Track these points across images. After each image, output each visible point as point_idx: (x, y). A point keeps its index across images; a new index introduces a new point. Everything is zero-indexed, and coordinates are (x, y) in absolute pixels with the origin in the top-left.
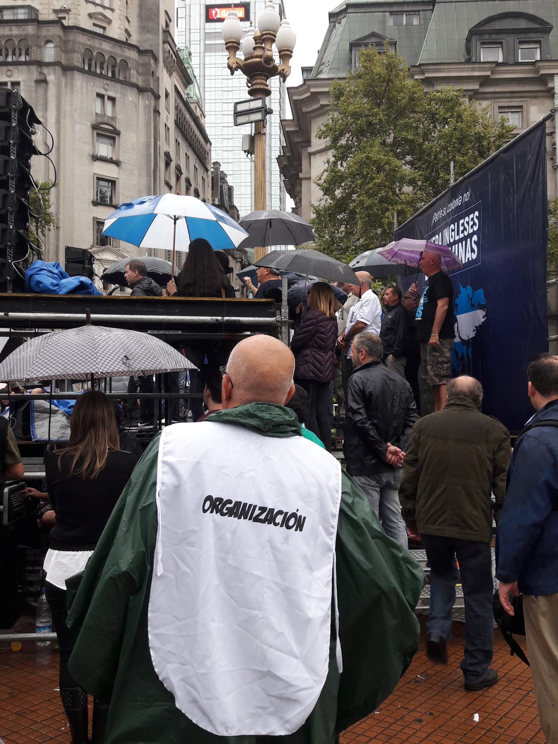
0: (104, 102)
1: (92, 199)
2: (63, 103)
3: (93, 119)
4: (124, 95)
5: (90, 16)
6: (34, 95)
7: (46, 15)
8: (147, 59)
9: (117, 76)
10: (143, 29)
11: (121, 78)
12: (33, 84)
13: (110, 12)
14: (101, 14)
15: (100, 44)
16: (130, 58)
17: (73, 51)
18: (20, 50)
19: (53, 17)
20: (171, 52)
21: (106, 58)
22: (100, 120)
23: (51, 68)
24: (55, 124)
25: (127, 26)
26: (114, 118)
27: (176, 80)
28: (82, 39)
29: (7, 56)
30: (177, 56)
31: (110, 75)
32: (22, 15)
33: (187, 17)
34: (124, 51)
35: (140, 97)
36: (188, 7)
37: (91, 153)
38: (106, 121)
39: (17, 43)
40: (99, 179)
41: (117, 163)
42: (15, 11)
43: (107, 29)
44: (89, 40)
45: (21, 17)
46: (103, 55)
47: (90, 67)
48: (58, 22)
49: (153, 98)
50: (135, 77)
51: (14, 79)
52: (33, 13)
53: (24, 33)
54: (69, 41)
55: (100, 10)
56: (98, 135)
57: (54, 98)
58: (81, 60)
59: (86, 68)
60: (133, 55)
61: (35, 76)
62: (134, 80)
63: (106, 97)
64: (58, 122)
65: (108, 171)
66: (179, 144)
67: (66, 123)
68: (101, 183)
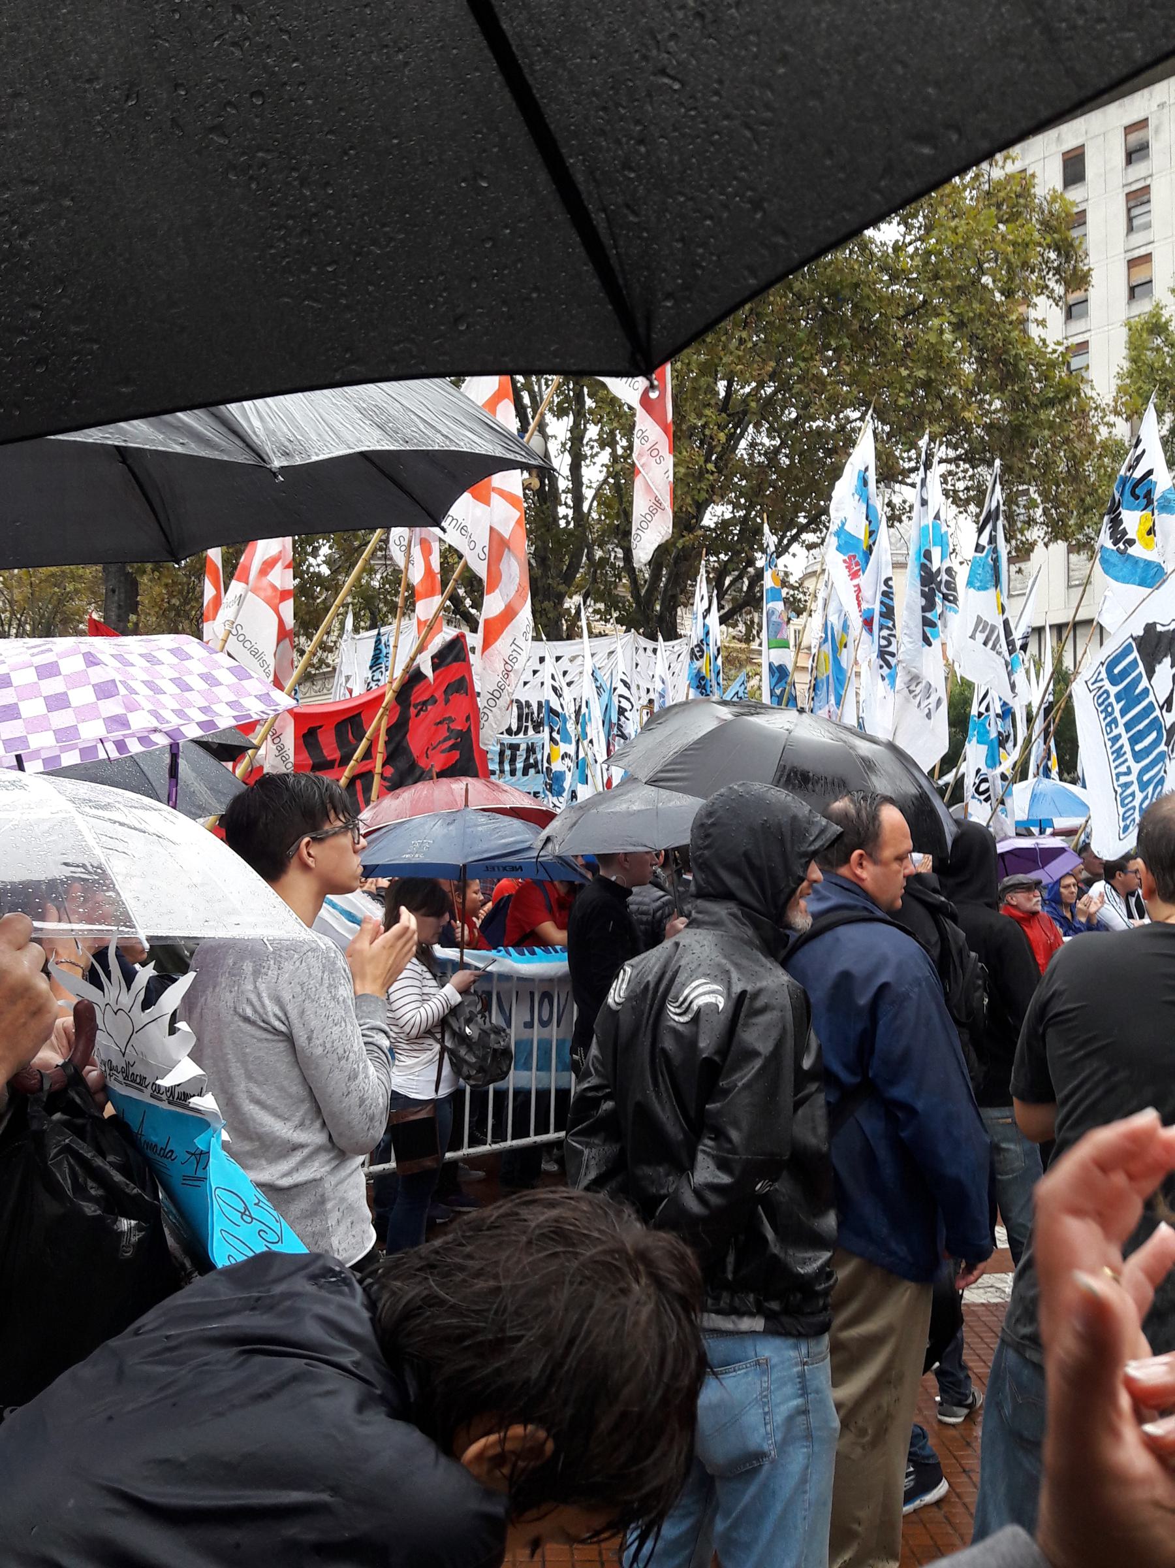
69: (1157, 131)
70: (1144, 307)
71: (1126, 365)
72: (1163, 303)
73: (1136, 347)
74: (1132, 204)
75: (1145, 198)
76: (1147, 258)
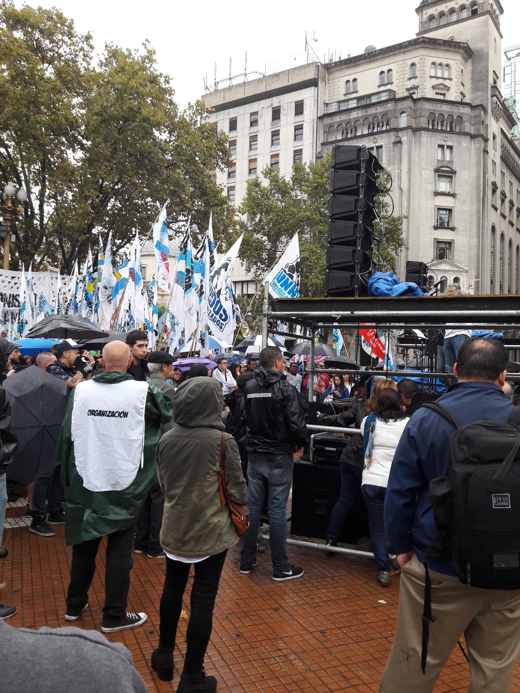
0: (444, 151)
1: (433, 225)
2: (413, 156)
3: (435, 165)
4: (459, 143)
5: (434, 87)
6: (392, 153)
7: (401, 93)
8: (477, 112)
9: (454, 129)
10: (475, 89)
11: (457, 131)
12: (391, 146)
13: (449, 81)
14: (442, 84)
15: (441, 107)
16: (464, 113)
17: (421, 116)
18: (383, 122)
19: (406, 94)
20: (498, 103)
21: (446, 117)
22: (440, 165)
23: (405, 131)
24: (407, 172)
25: (462, 89)
26: (451, 162)
27: (503, 124)
28: (428, 106)
29: (374, 128)
30: (503, 105)
31: (448, 129)
32: (384, 97)
33: (513, 73)
34: (460, 109)
35: (472, 142)
36: (513, 65)
37: (434, 190)
38: (445, 165)
39: (380, 118)
40: (439, 209)
41: (453, 196)
42: (380, 95)
43: (446, 95)
44: (432, 106)
45: (383, 99)
46: (444, 116)
47: (433, 125)
48: (410, 97)
49: (483, 141)
50: (468, 128)
51: (377, 144)
52: (392, 94)
53: (386, 109)
54: (418, 109)
55: (441, 81)
56: (439, 176)
57: (407, 154)
58: (426, 122)
59: (431, 127)
60: (467, 110)
61: (393, 139)
62: (467, 130)
63: (445, 147)
64: (409, 171)
65: (446, 202)
66: (504, 174)
67: (415, 170)
68: (441, 212)
69: (261, 116)
70: (253, 177)
71: (246, 196)
72: (259, 176)
73: (250, 191)
74: (251, 140)
75: (256, 139)
76: (255, 160)
